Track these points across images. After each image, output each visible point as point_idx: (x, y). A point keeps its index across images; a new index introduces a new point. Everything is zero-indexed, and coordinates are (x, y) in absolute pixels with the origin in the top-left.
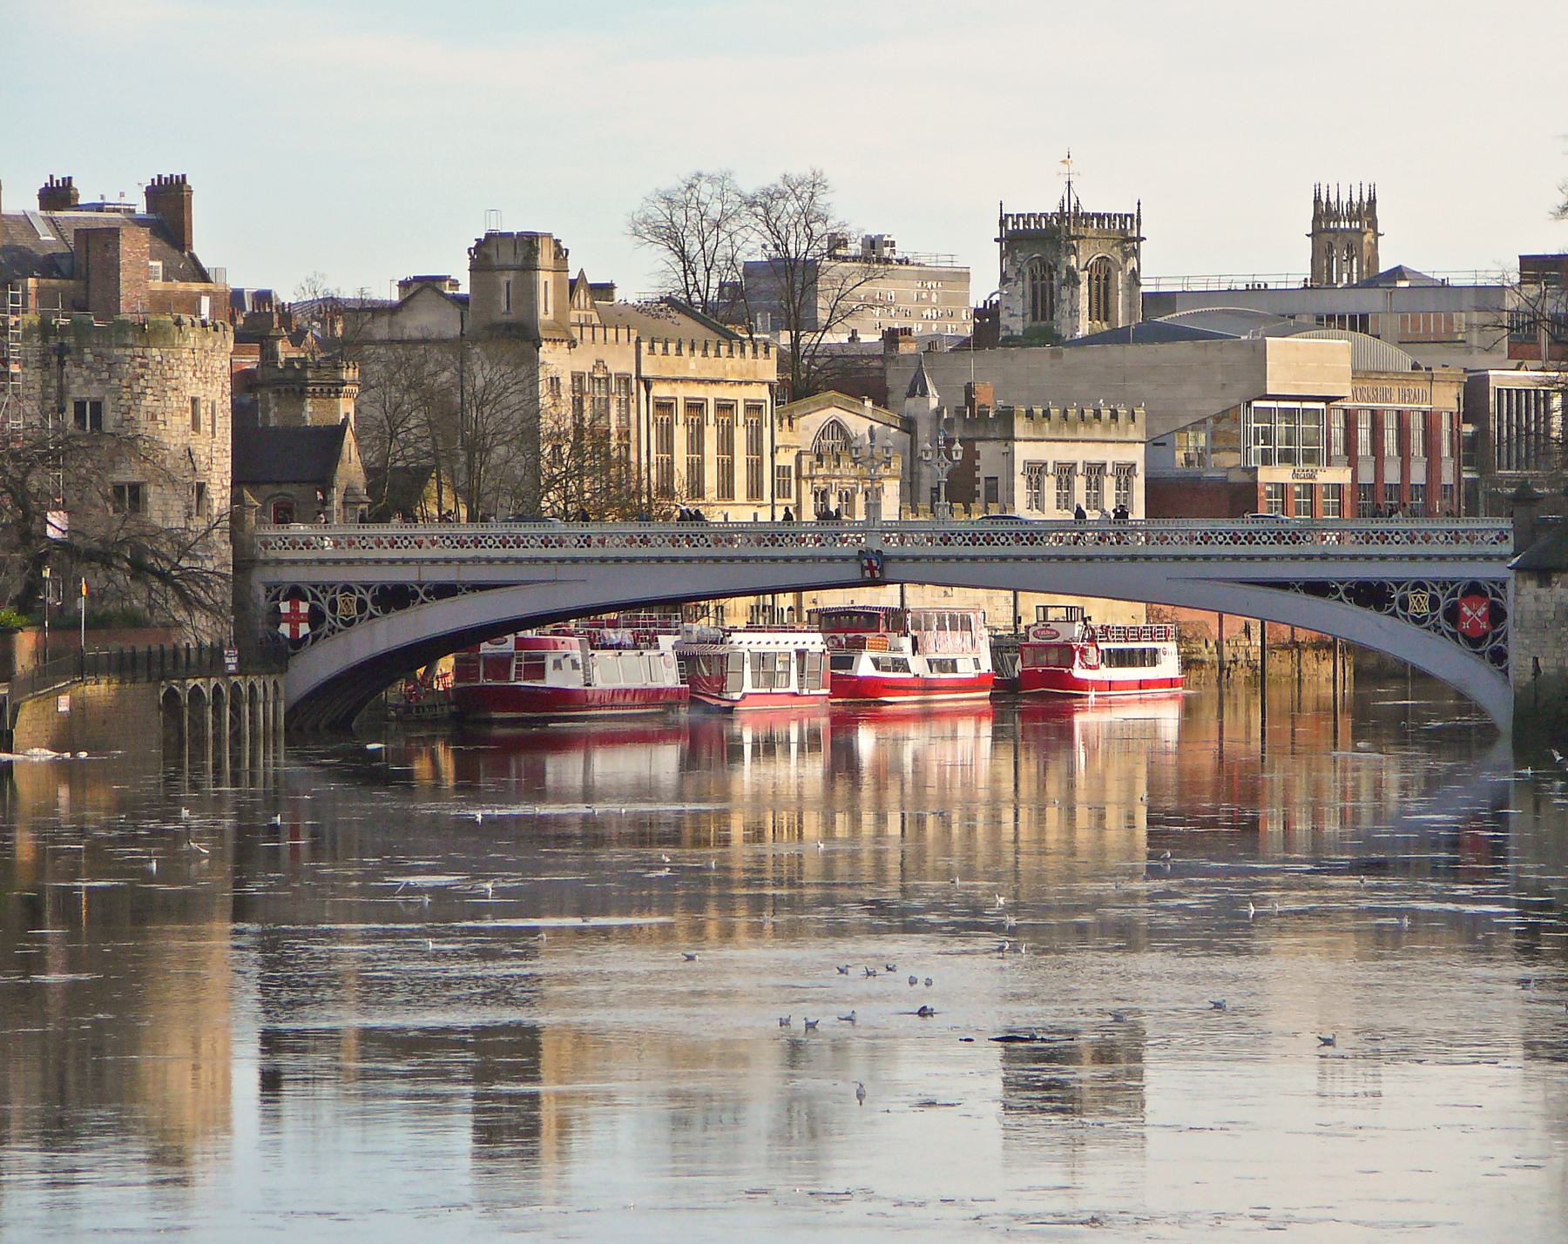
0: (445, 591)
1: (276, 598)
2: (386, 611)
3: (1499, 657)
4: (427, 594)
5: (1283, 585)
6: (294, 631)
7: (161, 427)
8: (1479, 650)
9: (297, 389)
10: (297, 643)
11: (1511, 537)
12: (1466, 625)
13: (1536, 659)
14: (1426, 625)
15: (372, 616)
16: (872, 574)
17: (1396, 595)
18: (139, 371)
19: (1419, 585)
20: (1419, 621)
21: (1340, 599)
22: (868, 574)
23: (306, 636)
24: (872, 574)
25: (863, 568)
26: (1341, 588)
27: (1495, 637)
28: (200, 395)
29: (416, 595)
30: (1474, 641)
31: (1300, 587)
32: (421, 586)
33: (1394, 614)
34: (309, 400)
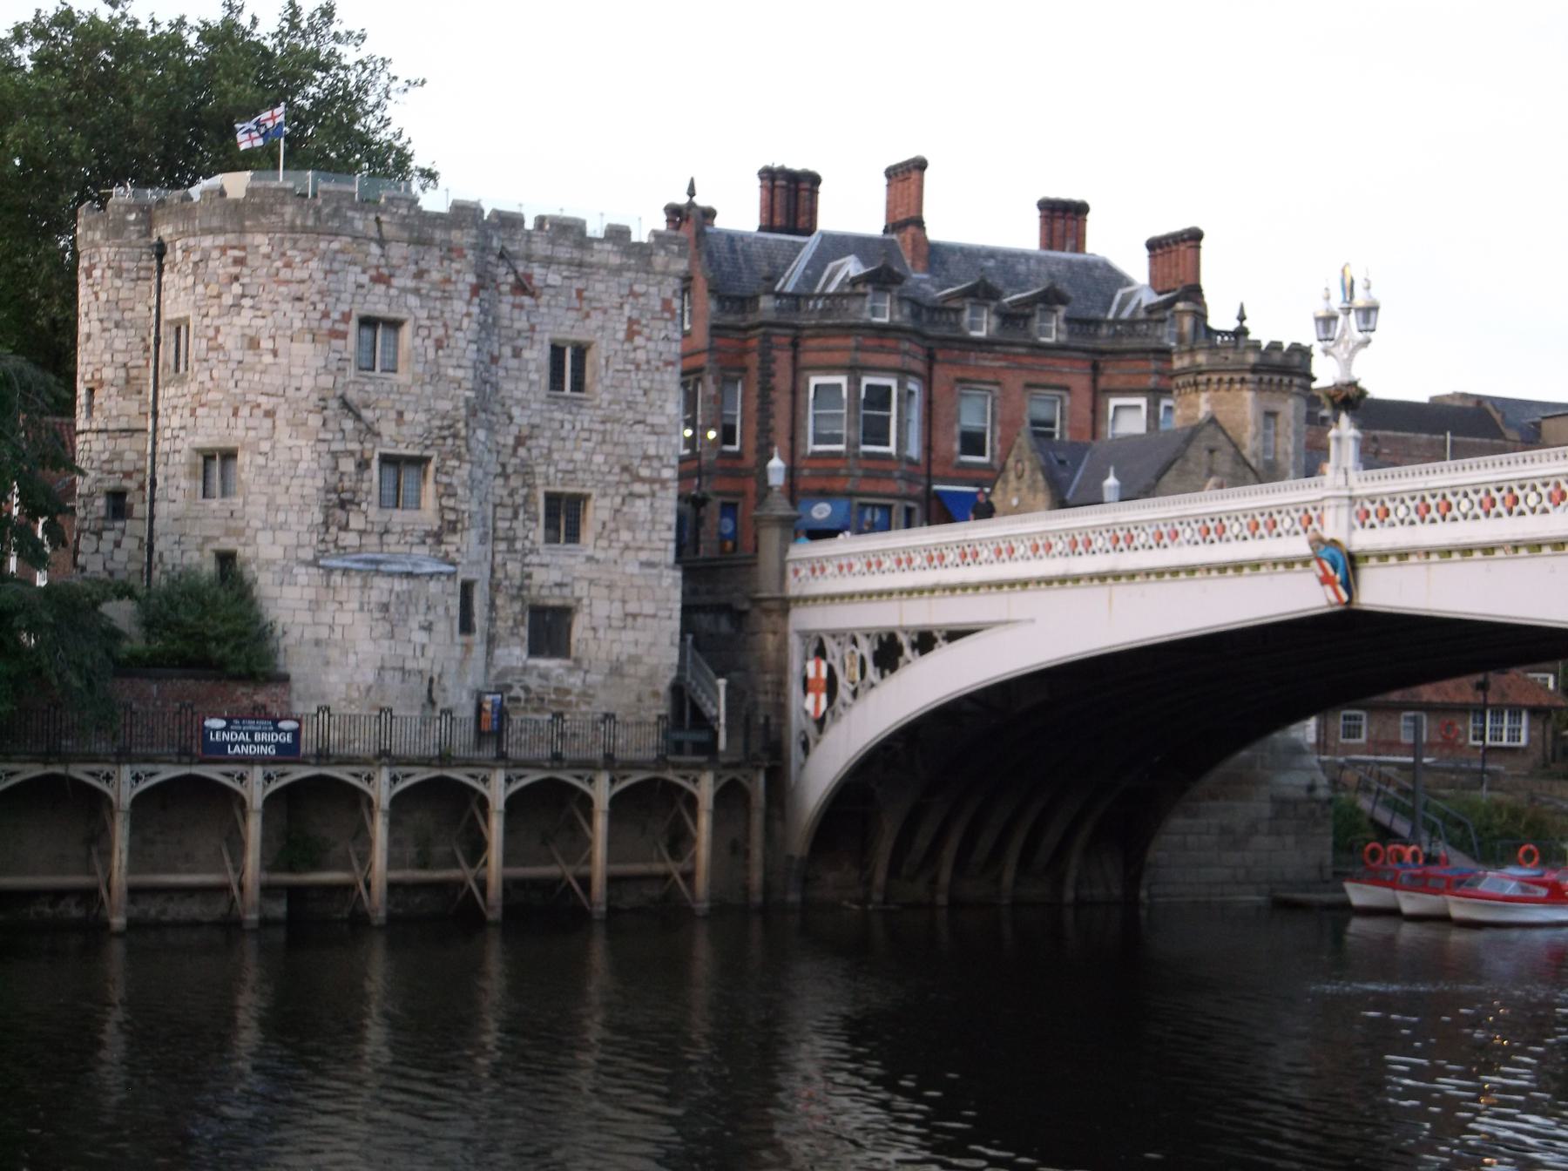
0: (925, 642)
1: (807, 659)
2: (882, 676)
4: (914, 646)
6: (817, 703)
7: (268, 359)
9: (1192, 380)
10: (820, 723)
15: (872, 685)
18: (235, 270)
22: (1333, 598)
23: (824, 714)
25: (1325, 580)
28: (412, 309)
29: (899, 650)
32: (906, 632)
34: (1204, 397)
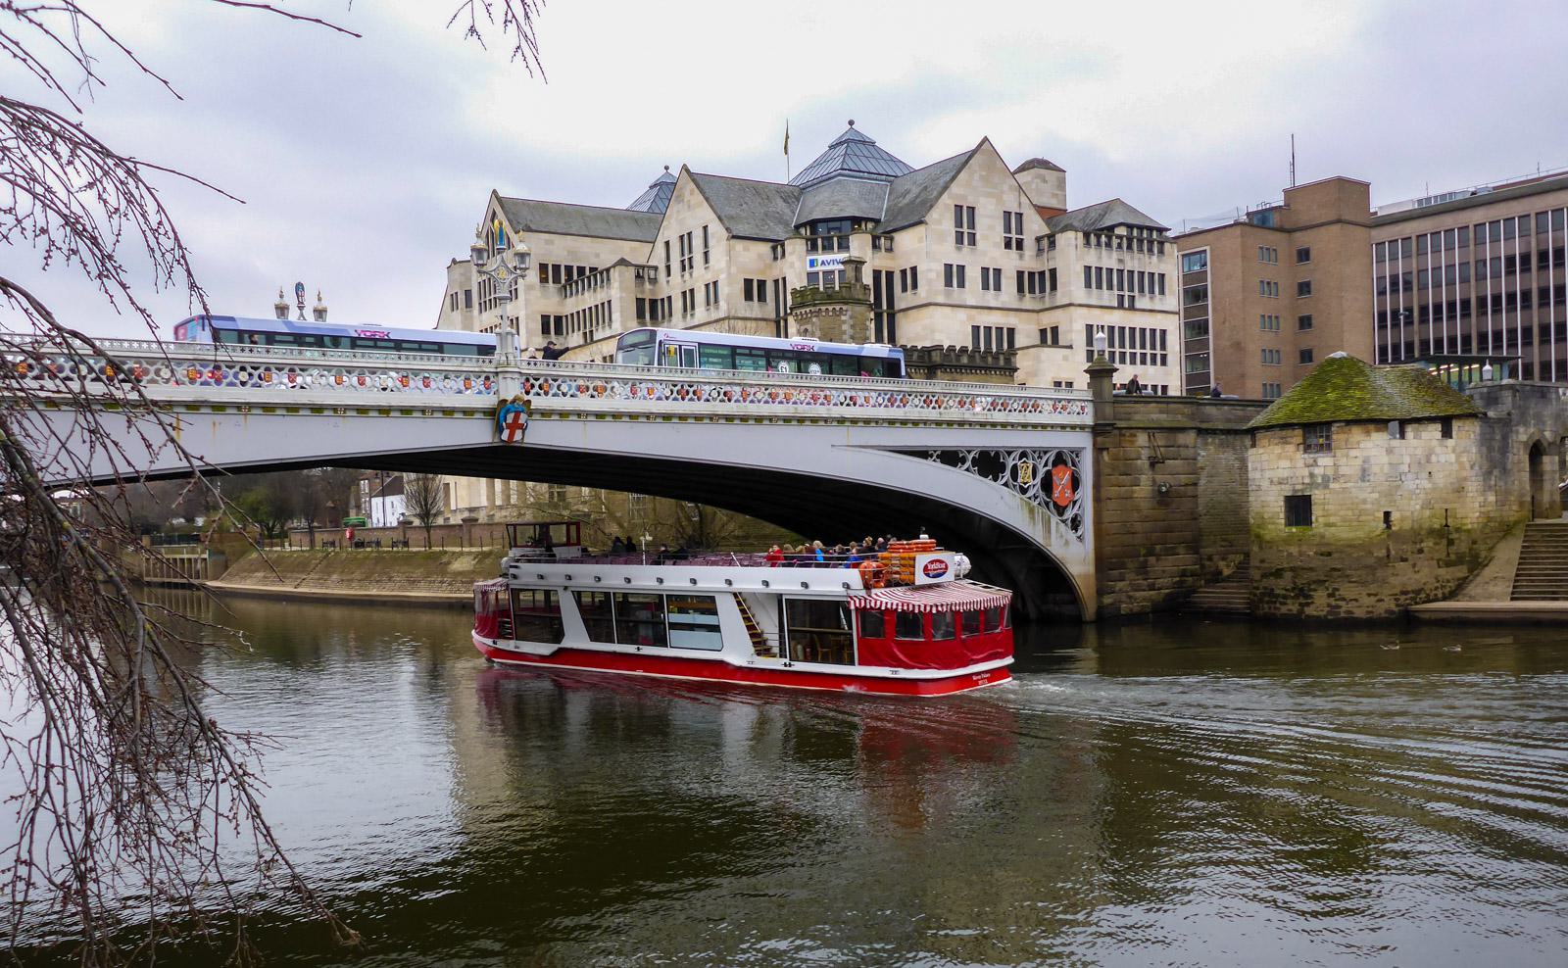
3: (1075, 524)
5: (923, 454)
8: (1064, 518)
11: (1089, 409)
12: (1056, 494)
13: (1387, 514)
14: (1028, 495)
16: (511, 435)
17: (1010, 463)
19: (1023, 455)
20: (1024, 491)
21: (967, 470)
22: (505, 436)
24: (511, 435)
26: (970, 457)
27: (1075, 503)
30: (1060, 510)
31: (938, 457)
33: (1006, 484)
